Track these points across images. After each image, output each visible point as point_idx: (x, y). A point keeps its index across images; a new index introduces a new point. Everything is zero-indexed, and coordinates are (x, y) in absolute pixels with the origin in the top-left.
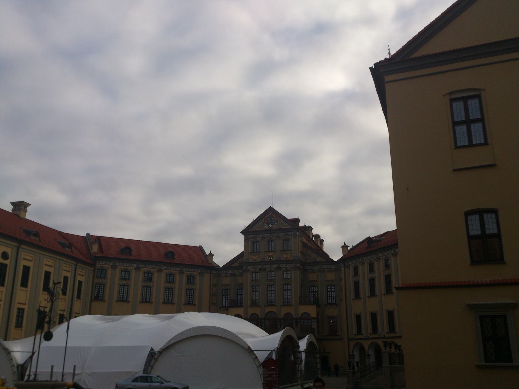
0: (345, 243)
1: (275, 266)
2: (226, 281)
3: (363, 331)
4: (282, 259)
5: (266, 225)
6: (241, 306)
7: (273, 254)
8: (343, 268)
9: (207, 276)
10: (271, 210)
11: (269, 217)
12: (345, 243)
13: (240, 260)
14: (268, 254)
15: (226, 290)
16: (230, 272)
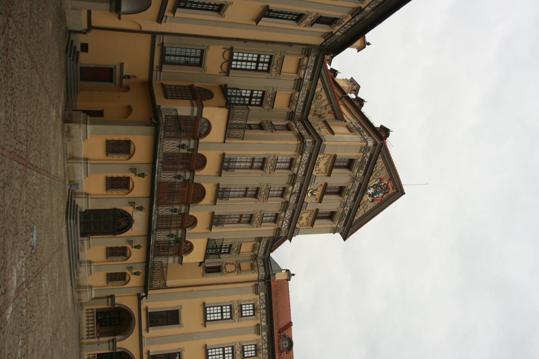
0: (293, 275)
1: (293, 200)
2: (290, 65)
3: (154, 332)
4: (302, 212)
5: (376, 183)
6: (227, 136)
7: (318, 196)
8: (254, 276)
9: (318, 41)
10: (399, 192)
11: (387, 187)
12: (293, 275)
13: (324, 97)
14: (320, 189)
15: (269, 63)
16: (308, 77)
